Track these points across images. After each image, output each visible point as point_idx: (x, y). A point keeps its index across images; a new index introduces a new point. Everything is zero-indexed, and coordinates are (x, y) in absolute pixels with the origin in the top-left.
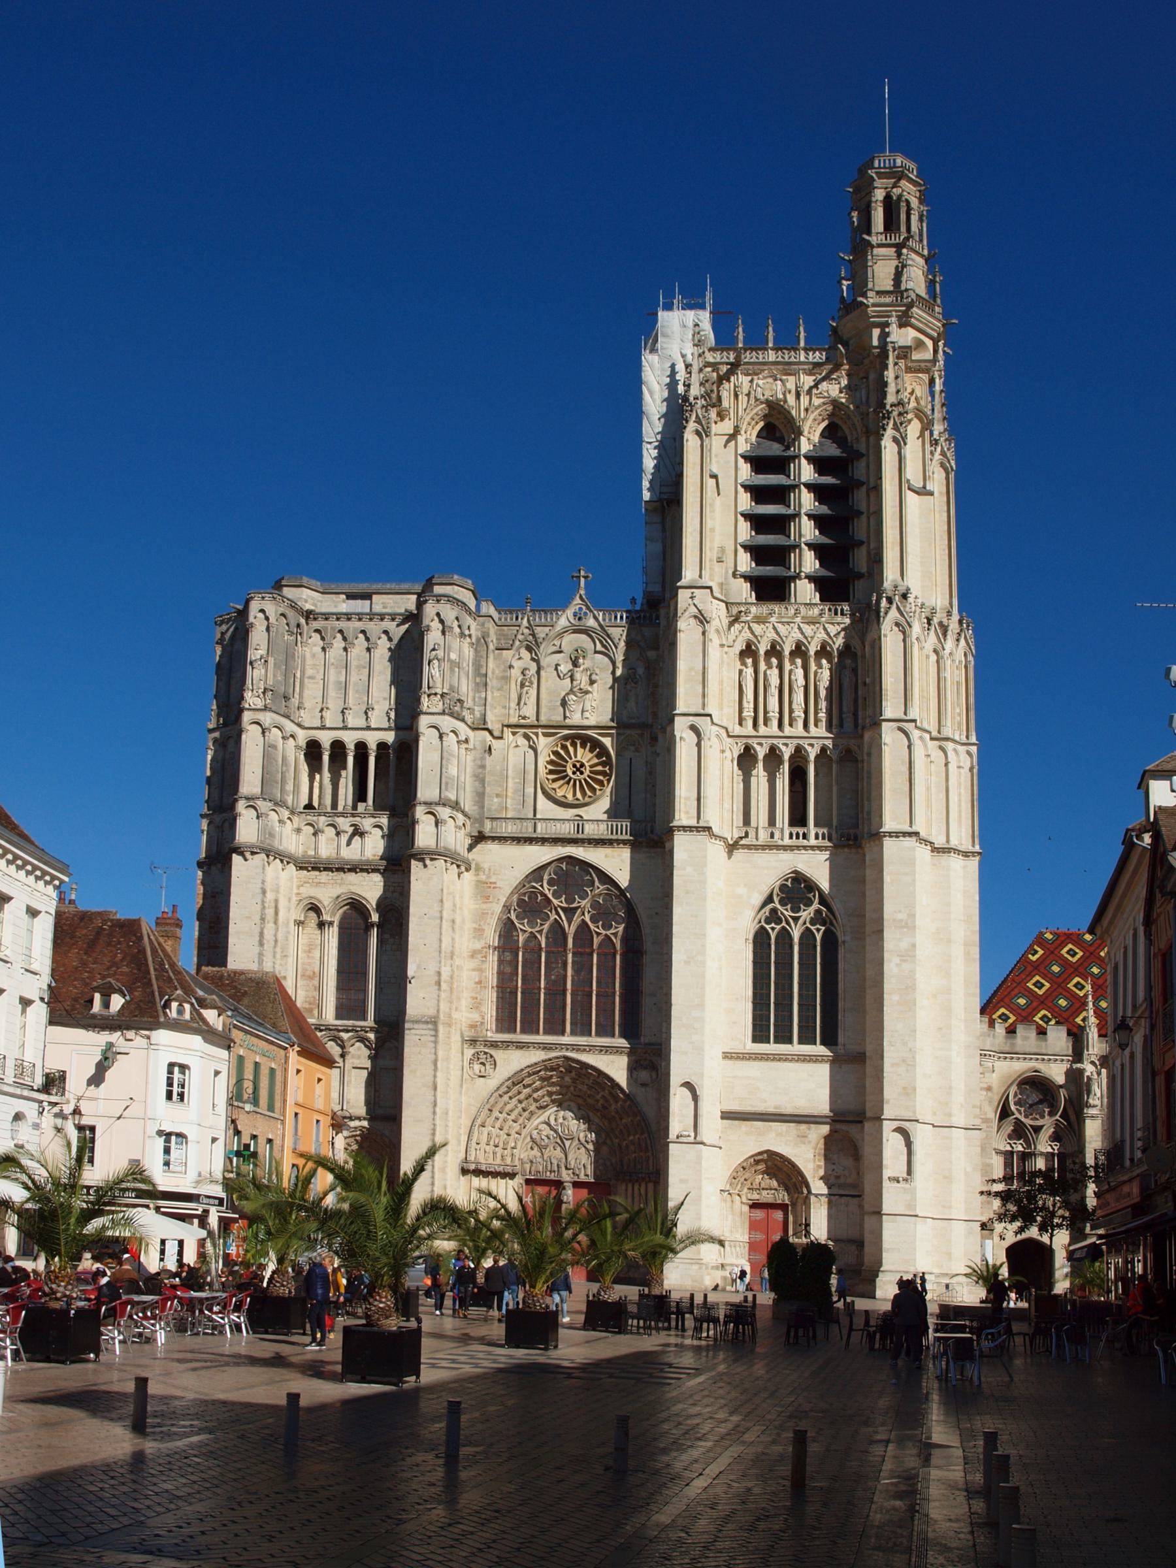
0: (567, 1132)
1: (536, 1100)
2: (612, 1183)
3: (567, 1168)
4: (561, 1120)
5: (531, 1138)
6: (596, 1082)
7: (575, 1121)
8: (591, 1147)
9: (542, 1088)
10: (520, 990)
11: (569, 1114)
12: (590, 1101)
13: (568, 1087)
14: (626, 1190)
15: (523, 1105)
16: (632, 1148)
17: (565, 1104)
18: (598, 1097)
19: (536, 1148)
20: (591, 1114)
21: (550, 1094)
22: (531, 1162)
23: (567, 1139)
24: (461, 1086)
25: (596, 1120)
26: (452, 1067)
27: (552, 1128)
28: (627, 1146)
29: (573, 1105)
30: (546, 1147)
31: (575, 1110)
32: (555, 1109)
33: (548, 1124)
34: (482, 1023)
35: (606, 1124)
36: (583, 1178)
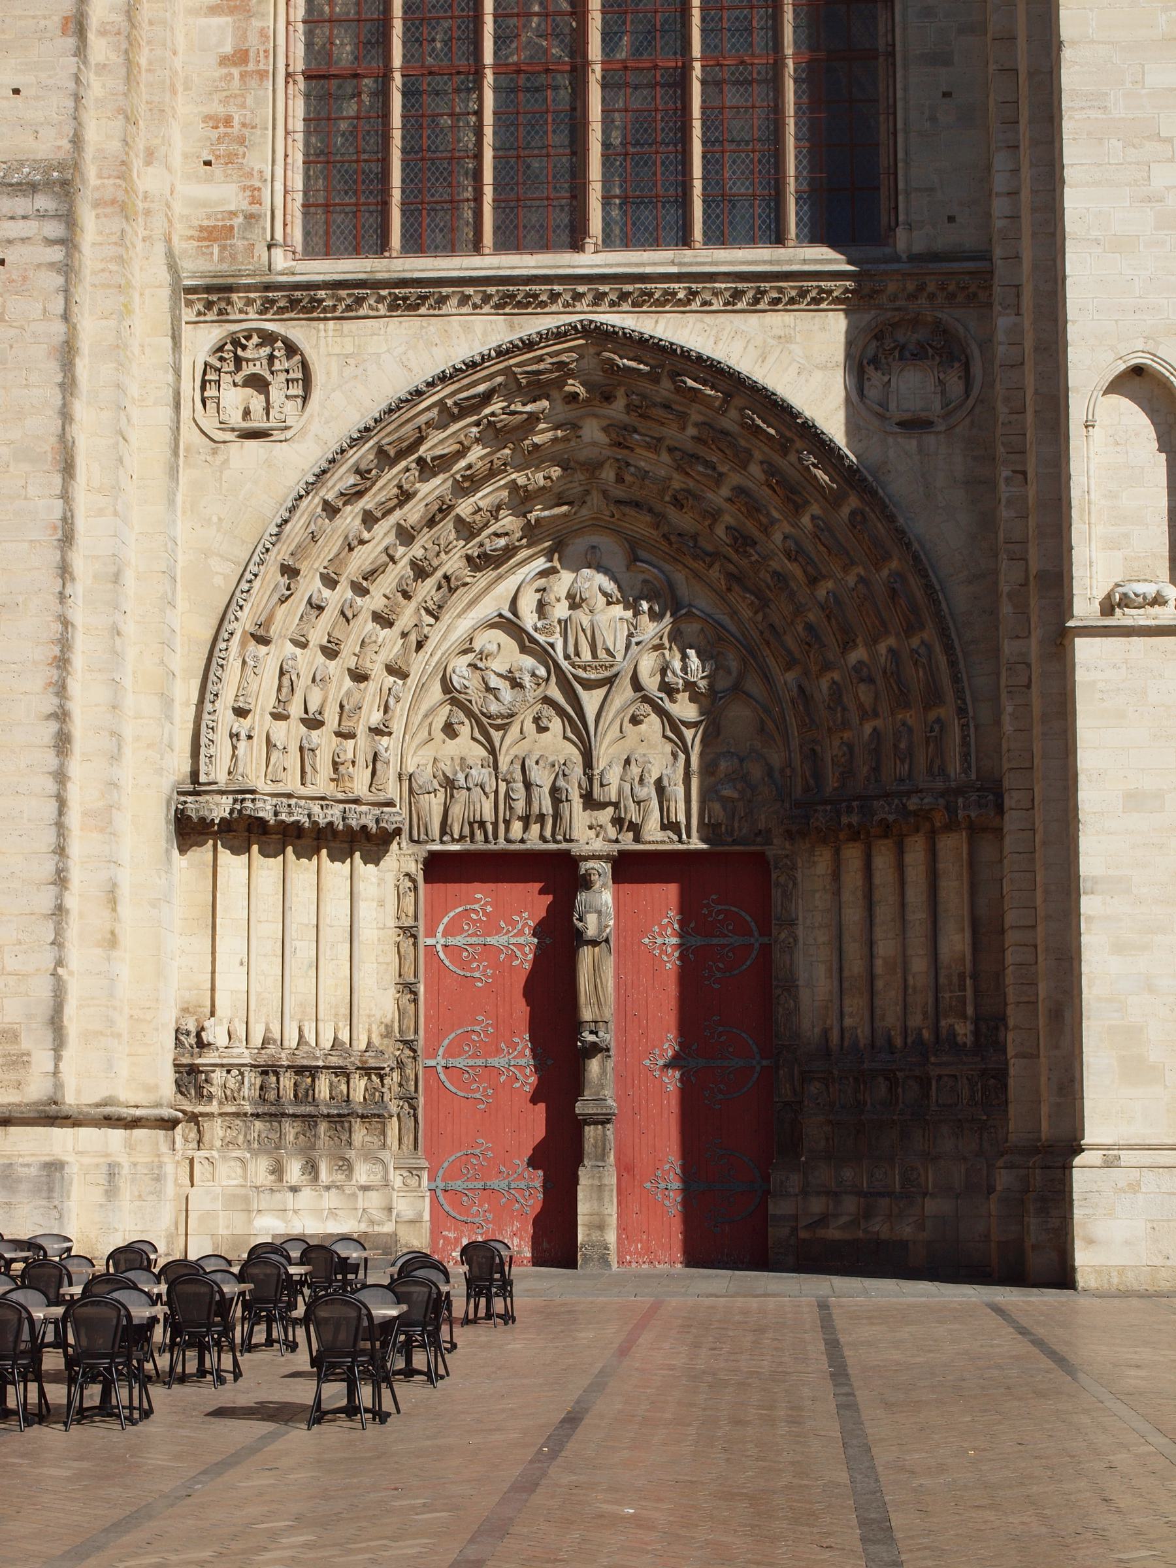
0: (586, 655)
1: (466, 530)
2: (776, 849)
3: (590, 802)
4: (561, 610)
5: (447, 686)
6: (712, 435)
7: (618, 611)
8: (685, 709)
9: (492, 473)
10: (397, 80)
11: (595, 582)
12: (684, 520)
13: (592, 467)
14: (836, 875)
15: (417, 551)
16: (864, 693)
17: (579, 545)
18: (718, 497)
19: (465, 730)
20: (679, 577)
21: (521, 499)
22: (449, 784)
23: (589, 685)
24: (173, 472)
25: (703, 601)
26: (134, 390)
27: (526, 643)
28: (837, 691)
29: (607, 543)
30: (504, 722)
31: (618, 561)
32: (540, 563)
33: (509, 624)
34: (251, 218)
35: (746, 613)
36: (655, 836)
